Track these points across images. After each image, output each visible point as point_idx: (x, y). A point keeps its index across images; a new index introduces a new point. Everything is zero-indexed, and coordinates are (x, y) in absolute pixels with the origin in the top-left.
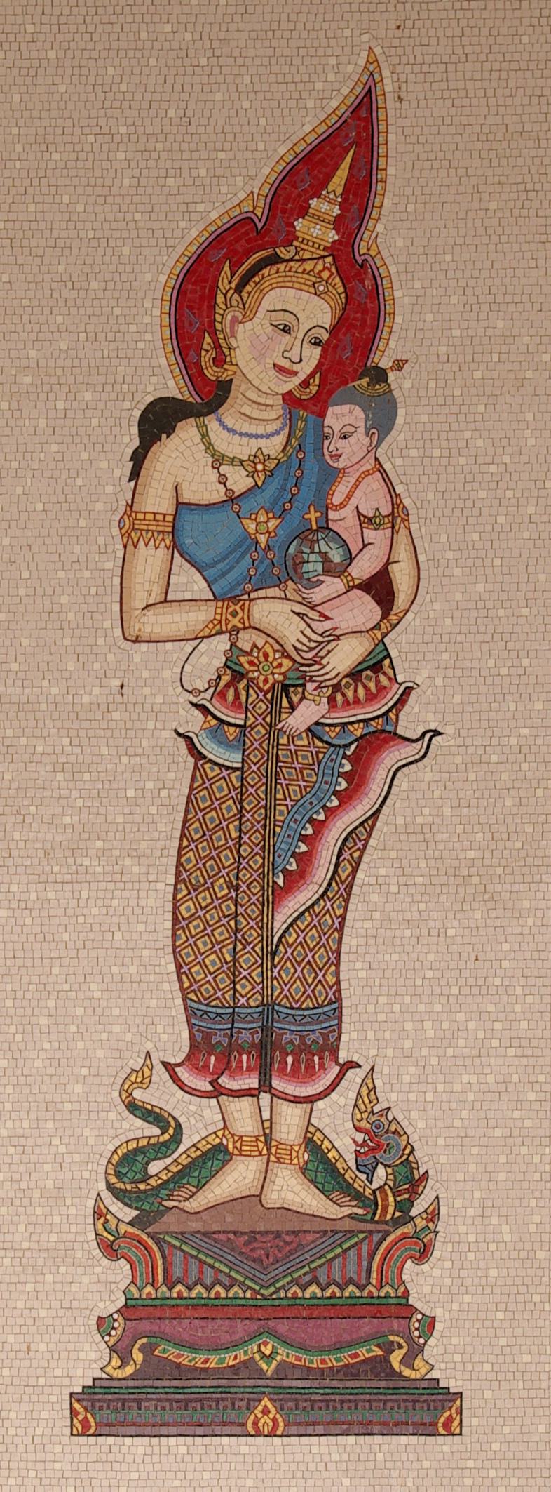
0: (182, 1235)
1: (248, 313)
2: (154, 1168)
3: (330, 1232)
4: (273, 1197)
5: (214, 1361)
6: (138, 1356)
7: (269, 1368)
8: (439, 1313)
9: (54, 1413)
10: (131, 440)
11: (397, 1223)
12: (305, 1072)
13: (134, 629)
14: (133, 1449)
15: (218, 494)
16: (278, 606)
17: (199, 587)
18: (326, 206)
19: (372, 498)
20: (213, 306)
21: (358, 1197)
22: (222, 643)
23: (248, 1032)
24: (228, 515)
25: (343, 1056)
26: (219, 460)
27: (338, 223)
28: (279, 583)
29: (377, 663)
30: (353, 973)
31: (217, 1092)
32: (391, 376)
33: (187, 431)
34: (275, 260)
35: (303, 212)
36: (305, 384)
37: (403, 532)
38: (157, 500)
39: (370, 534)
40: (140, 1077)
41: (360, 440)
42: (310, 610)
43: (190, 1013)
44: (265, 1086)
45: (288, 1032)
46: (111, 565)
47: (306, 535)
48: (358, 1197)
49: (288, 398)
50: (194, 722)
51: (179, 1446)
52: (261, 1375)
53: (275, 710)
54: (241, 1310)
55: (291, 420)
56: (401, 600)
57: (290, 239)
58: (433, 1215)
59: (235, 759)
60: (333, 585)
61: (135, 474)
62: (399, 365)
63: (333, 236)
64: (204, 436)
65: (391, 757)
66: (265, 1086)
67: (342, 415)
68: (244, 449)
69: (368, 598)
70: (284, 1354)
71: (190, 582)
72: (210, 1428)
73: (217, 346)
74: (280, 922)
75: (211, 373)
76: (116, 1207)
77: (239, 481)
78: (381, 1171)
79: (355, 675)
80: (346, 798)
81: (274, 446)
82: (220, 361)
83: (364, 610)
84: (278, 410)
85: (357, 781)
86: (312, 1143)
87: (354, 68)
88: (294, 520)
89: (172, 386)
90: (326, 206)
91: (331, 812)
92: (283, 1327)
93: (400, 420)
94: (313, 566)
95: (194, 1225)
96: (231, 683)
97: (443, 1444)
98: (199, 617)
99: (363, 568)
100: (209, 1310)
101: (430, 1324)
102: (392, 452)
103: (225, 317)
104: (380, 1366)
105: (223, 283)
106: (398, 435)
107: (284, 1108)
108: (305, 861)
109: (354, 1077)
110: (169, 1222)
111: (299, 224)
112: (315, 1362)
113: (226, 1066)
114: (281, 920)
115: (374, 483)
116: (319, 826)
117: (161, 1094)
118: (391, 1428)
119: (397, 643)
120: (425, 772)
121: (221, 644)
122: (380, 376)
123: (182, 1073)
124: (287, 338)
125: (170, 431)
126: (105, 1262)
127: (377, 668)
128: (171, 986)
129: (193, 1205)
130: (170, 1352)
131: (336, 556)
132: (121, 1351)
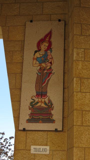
0: (35, 108)
1: (42, 45)
2: (33, 103)
3: (45, 108)
4: (42, 106)
5: (37, 117)
6: (31, 117)
7: (41, 118)
8: (54, 114)
9: (25, 121)
10: (34, 53)
11: (51, 108)
12: (44, 97)
13: (34, 66)
14: (31, 124)
15: (40, 57)
16: (44, 64)
17: (38, 63)
18: (48, 38)
19: (50, 57)
20: (40, 44)
21: (48, 106)
22: (40, 67)
23: (40, 94)
24: (40, 58)
25: (47, 95)
26: (40, 54)
27: (49, 39)
28: (44, 62)
29: (50, 68)
30: (48, 89)
31: (38, 98)
32: (52, 49)
33: (38, 52)
34: (44, 41)
35: (46, 38)
36: (46, 49)
37: (53, 60)
38: (35, 57)
39: (50, 59)
40: (32, 97)
41: (50, 53)
42: (46, 64)
43: (36, 92)
44: (41, 97)
45: (43, 94)
46: (32, 61)
47: (46, 59)
48: (48, 106)
49: (45, 50)
50: (37, 72)
51: (34, 124)
52: (40, 119)
53: (43, 71)
54: (39, 114)
55: (45, 52)
56: (52, 64)
57: (45, 40)
58: (53, 107)
59: (40, 75)
60: (48, 63)
61: (34, 55)
62: (53, 48)
63: (48, 40)
64: (39, 53)
65: (51, 74)
66: (41, 97)
67: (49, 51)
68: (42, 54)
69: (50, 64)
70: (42, 117)
71: (37, 63)
72: (36, 123)
73: (40, 47)
74: (43, 86)
75: (40, 49)
76: (30, 106)
77: (41, 56)
78: (50, 104)
79: (49, 69)
80: (48, 77)
81: (44, 53)
82: (40, 48)
83: (50, 64)
84: (44, 51)
85: (49, 76)
86: (45, 102)
87: (50, 29)
88: (45, 58)
89: (37, 50)
90: (48, 38)
91: (47, 78)
92: (42, 115)
93: (53, 52)
94: (46, 61)
95: (36, 107)
96: (40, 69)
97: (54, 124)
98: (38, 65)
99: (50, 61)
100: (37, 114)
101: (53, 115)
102: (52, 54)
103: (41, 45)
104: (49, 118)
105: (41, 43)
106: (52, 53)
107: (43, 99)
108: (45, 82)
109: (48, 97)
110: (34, 107)
111: (46, 39)
112: (44, 118)
113: (39, 96)
114: (43, 86)
115: (51, 56)
116: (46, 79)
117: (34, 98)
118: (50, 123)
119: (52, 67)
120: (54, 75)
121: (40, 67)
122: (51, 49)
123: (36, 97)
124: (45, 47)
125: (36, 52)
126: (29, 110)
127: (50, 68)
128: (35, 90)
129: (36, 106)
130: (34, 117)
131: (48, 61)
132: (30, 117)
